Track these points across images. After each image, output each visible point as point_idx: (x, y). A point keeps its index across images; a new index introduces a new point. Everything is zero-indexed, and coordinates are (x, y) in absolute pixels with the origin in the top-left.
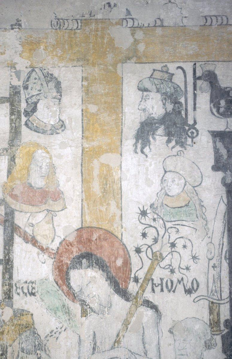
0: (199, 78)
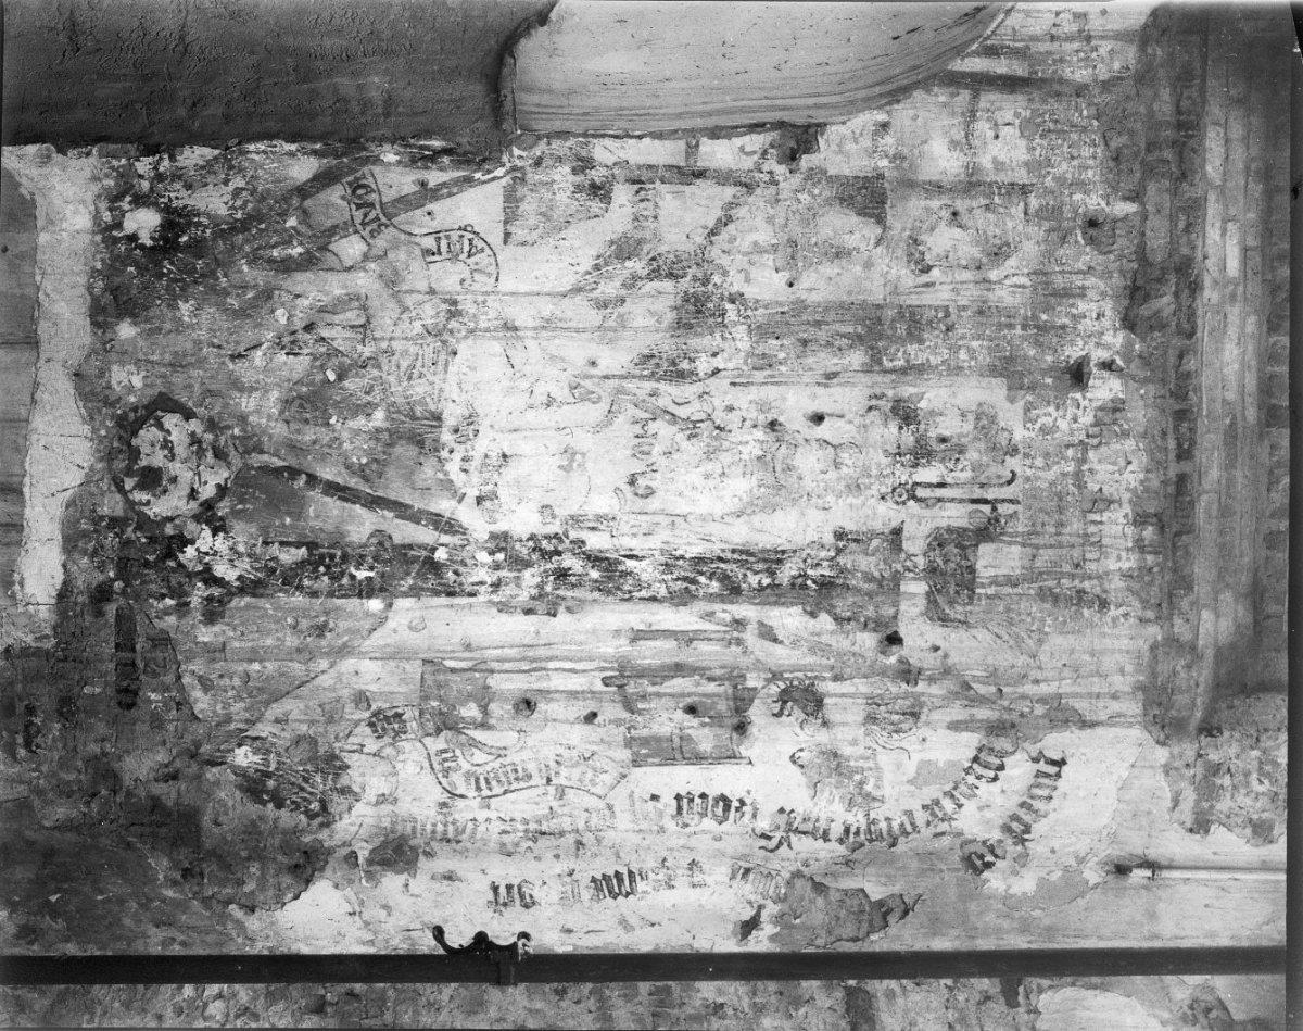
0: (994, 509)
